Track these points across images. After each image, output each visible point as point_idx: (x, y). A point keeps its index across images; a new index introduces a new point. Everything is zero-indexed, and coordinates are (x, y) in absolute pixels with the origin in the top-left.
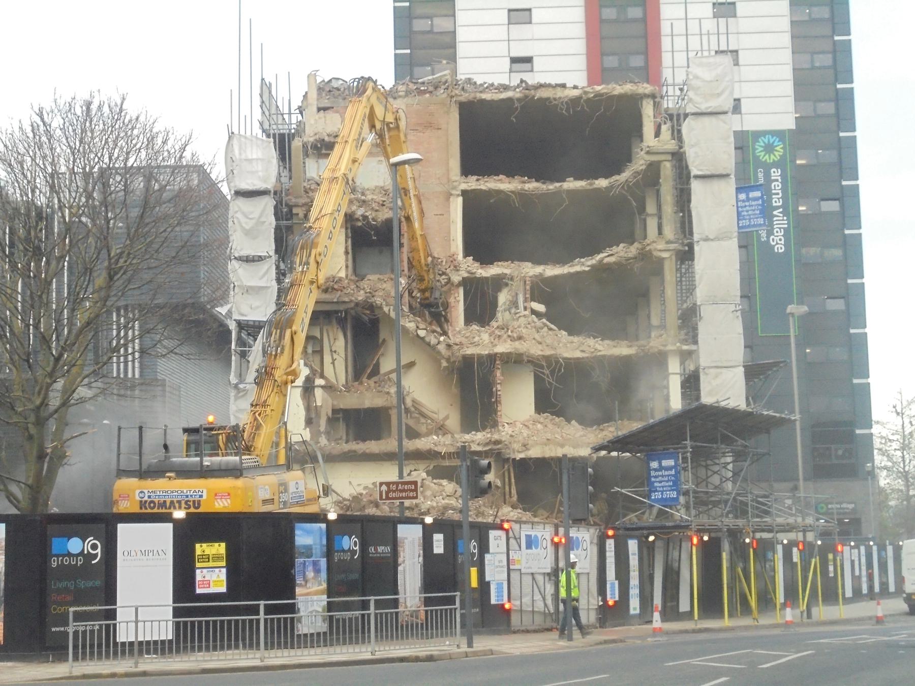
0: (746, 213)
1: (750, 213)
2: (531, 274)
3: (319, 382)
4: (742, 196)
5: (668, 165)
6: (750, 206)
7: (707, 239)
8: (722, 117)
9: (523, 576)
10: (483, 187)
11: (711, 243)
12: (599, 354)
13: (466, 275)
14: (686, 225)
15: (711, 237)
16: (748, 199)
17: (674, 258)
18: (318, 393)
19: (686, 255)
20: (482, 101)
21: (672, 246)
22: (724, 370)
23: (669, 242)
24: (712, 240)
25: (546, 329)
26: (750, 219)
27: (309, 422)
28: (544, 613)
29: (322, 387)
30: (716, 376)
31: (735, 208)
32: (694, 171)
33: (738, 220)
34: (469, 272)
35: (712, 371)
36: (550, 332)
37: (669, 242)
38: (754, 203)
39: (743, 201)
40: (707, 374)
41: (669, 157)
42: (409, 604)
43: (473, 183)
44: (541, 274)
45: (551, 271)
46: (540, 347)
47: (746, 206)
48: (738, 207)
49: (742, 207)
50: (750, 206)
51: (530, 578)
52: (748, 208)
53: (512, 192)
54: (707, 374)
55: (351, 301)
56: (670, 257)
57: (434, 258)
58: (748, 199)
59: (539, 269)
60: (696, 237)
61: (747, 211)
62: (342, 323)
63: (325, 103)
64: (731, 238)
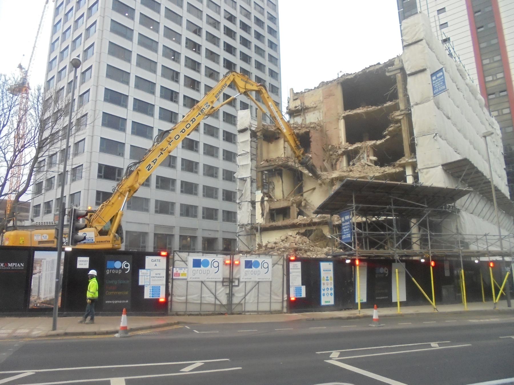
0: (436, 86)
1: (438, 85)
2: (370, 145)
3: (266, 198)
4: (434, 78)
5: (399, 75)
6: (438, 82)
7: (417, 104)
8: (420, 43)
9: (189, 283)
10: (351, 113)
11: (420, 106)
12: (386, 173)
13: (343, 150)
14: (408, 100)
15: (418, 102)
16: (437, 78)
17: (405, 118)
18: (265, 203)
19: (409, 116)
20: (348, 79)
21: (403, 112)
22: (431, 169)
23: (402, 110)
24: (420, 104)
25: (366, 166)
26: (438, 88)
27: (263, 215)
28: (215, 304)
29: (267, 200)
30: (427, 173)
31: (431, 86)
32: (408, 72)
33: (434, 90)
34: (344, 148)
35: (425, 170)
36: (369, 167)
37: (402, 110)
38: (439, 79)
39: (435, 80)
40: (422, 173)
41: (399, 71)
42: (42, 296)
43: (348, 113)
44: (374, 144)
45: (379, 142)
46: (359, 173)
47: (436, 82)
48: (433, 84)
49: (434, 83)
50: (438, 82)
51: (200, 283)
52: (437, 83)
53: (363, 113)
54: (422, 173)
55: (275, 165)
56: (403, 117)
57: (332, 146)
58: (437, 78)
59: (373, 142)
60: (412, 104)
61: (437, 85)
62: (280, 174)
63: (295, 98)
64: (429, 101)
